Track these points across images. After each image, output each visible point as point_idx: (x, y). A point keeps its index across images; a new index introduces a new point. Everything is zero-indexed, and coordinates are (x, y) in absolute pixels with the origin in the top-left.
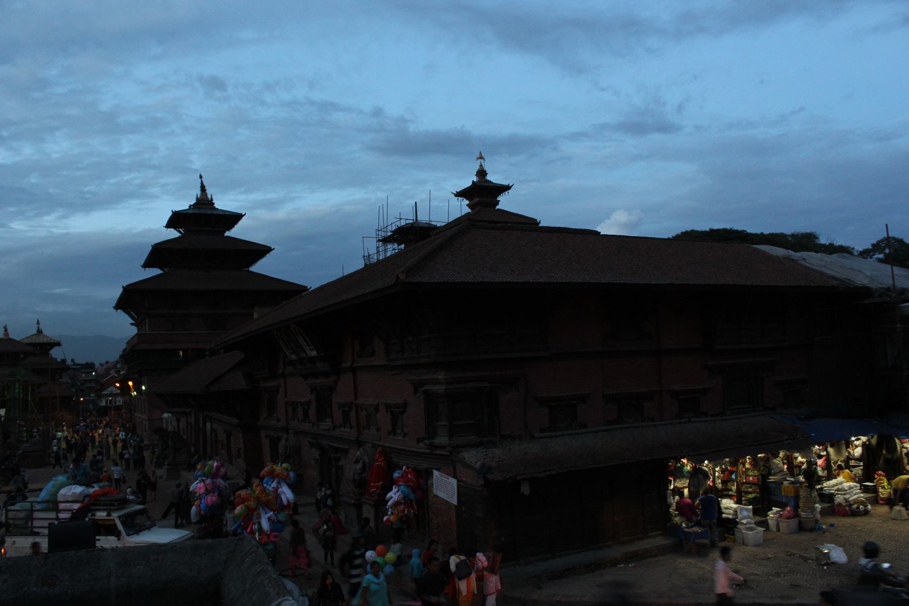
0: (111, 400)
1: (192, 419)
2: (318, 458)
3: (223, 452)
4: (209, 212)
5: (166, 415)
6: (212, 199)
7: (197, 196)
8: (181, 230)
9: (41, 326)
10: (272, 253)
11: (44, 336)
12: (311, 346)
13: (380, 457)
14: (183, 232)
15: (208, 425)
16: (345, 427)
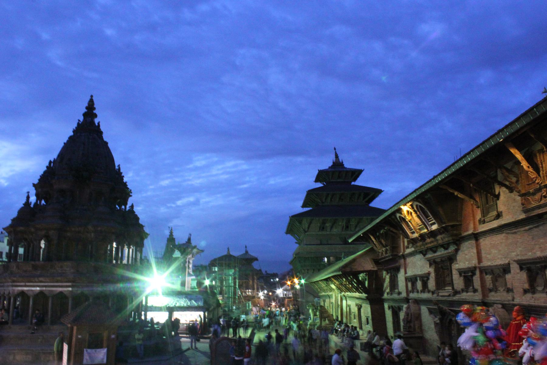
0: (286, 295)
1: (333, 300)
2: (438, 321)
3: (355, 321)
4: (340, 170)
5: (316, 299)
6: (342, 162)
7: (333, 160)
8: (325, 183)
9: (247, 249)
10: (382, 193)
11: (249, 254)
12: (433, 220)
13: (518, 316)
14: (325, 184)
15: (344, 302)
16: (467, 292)
